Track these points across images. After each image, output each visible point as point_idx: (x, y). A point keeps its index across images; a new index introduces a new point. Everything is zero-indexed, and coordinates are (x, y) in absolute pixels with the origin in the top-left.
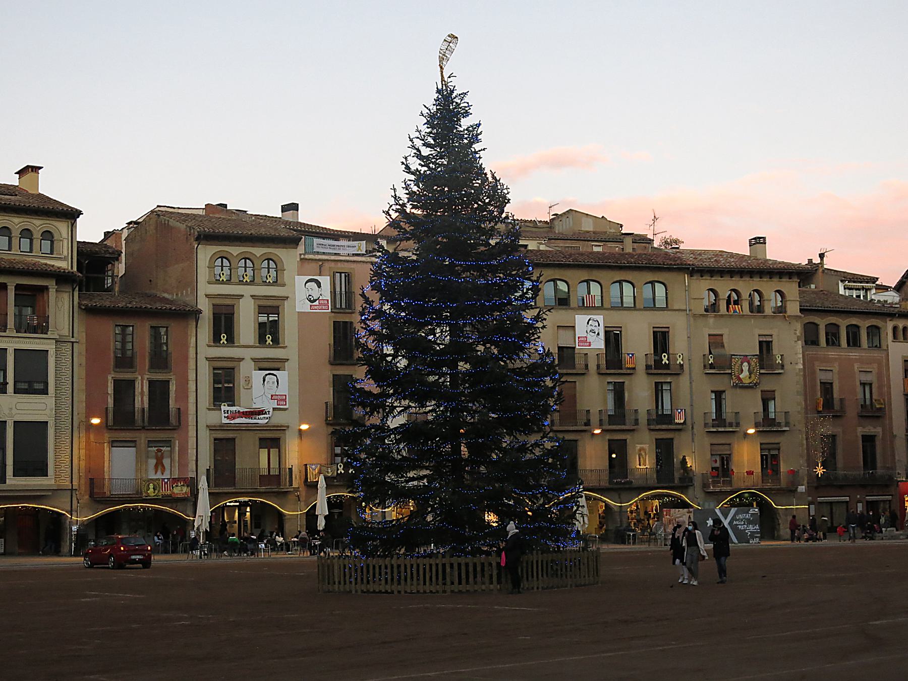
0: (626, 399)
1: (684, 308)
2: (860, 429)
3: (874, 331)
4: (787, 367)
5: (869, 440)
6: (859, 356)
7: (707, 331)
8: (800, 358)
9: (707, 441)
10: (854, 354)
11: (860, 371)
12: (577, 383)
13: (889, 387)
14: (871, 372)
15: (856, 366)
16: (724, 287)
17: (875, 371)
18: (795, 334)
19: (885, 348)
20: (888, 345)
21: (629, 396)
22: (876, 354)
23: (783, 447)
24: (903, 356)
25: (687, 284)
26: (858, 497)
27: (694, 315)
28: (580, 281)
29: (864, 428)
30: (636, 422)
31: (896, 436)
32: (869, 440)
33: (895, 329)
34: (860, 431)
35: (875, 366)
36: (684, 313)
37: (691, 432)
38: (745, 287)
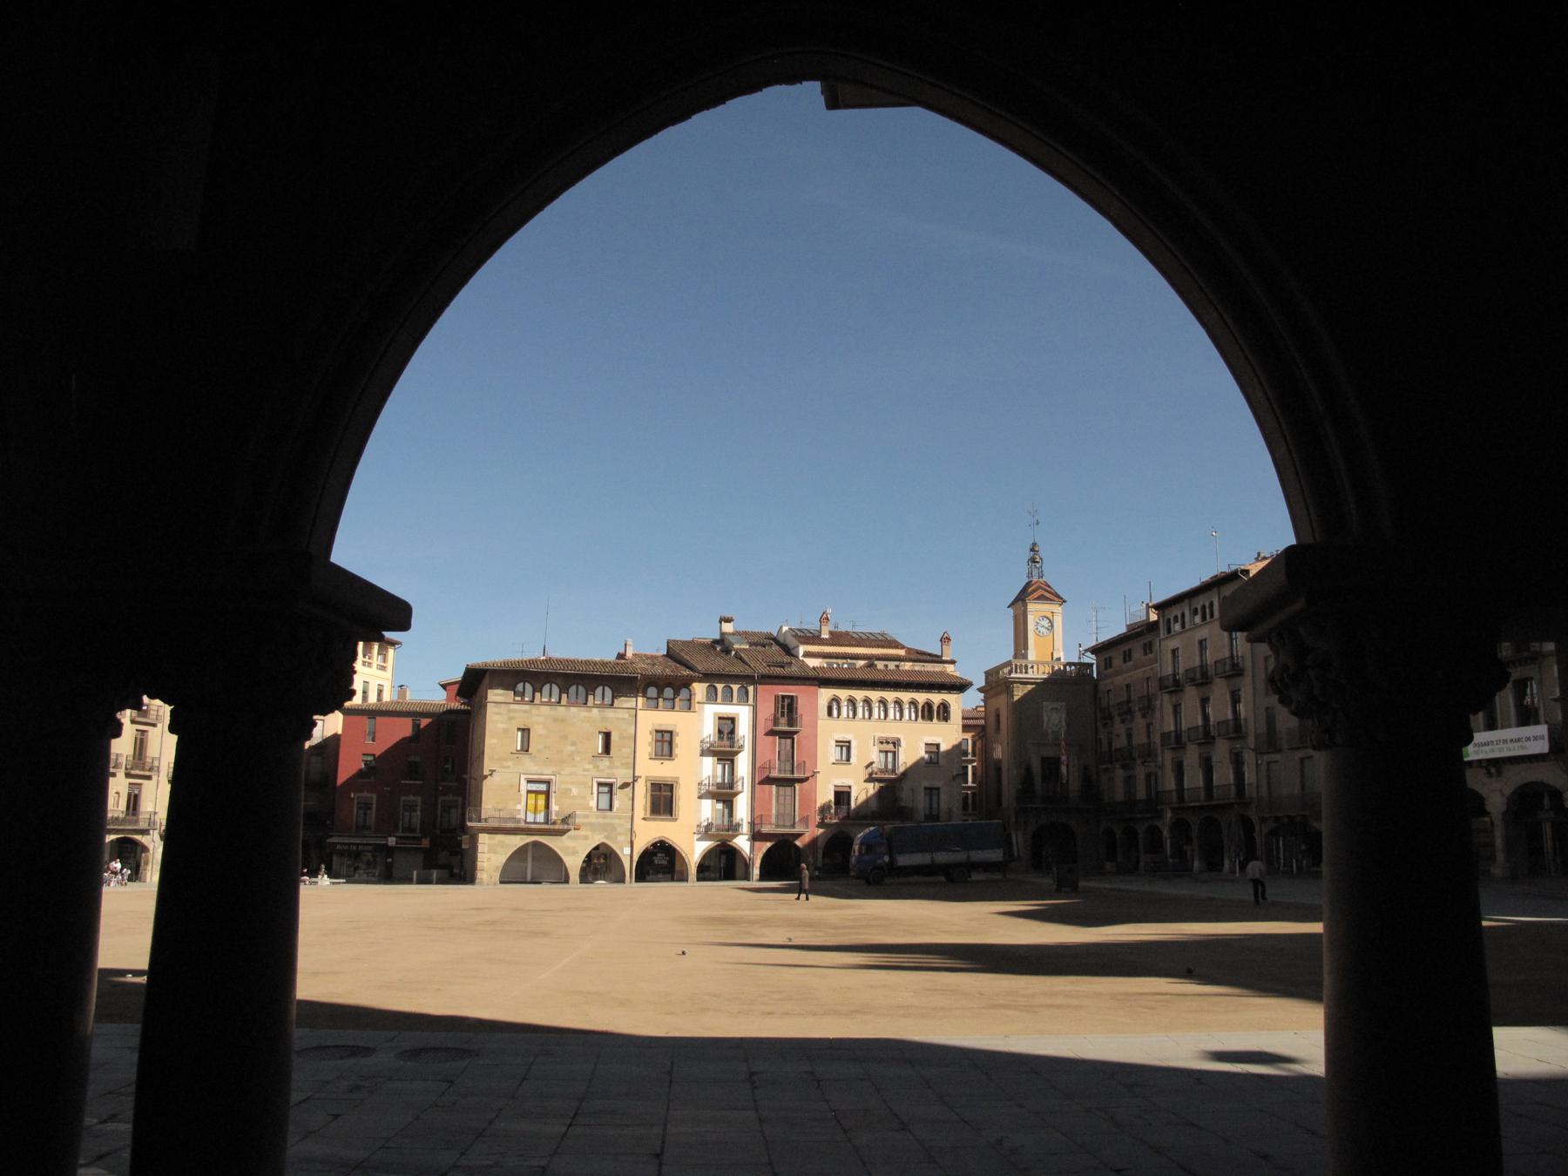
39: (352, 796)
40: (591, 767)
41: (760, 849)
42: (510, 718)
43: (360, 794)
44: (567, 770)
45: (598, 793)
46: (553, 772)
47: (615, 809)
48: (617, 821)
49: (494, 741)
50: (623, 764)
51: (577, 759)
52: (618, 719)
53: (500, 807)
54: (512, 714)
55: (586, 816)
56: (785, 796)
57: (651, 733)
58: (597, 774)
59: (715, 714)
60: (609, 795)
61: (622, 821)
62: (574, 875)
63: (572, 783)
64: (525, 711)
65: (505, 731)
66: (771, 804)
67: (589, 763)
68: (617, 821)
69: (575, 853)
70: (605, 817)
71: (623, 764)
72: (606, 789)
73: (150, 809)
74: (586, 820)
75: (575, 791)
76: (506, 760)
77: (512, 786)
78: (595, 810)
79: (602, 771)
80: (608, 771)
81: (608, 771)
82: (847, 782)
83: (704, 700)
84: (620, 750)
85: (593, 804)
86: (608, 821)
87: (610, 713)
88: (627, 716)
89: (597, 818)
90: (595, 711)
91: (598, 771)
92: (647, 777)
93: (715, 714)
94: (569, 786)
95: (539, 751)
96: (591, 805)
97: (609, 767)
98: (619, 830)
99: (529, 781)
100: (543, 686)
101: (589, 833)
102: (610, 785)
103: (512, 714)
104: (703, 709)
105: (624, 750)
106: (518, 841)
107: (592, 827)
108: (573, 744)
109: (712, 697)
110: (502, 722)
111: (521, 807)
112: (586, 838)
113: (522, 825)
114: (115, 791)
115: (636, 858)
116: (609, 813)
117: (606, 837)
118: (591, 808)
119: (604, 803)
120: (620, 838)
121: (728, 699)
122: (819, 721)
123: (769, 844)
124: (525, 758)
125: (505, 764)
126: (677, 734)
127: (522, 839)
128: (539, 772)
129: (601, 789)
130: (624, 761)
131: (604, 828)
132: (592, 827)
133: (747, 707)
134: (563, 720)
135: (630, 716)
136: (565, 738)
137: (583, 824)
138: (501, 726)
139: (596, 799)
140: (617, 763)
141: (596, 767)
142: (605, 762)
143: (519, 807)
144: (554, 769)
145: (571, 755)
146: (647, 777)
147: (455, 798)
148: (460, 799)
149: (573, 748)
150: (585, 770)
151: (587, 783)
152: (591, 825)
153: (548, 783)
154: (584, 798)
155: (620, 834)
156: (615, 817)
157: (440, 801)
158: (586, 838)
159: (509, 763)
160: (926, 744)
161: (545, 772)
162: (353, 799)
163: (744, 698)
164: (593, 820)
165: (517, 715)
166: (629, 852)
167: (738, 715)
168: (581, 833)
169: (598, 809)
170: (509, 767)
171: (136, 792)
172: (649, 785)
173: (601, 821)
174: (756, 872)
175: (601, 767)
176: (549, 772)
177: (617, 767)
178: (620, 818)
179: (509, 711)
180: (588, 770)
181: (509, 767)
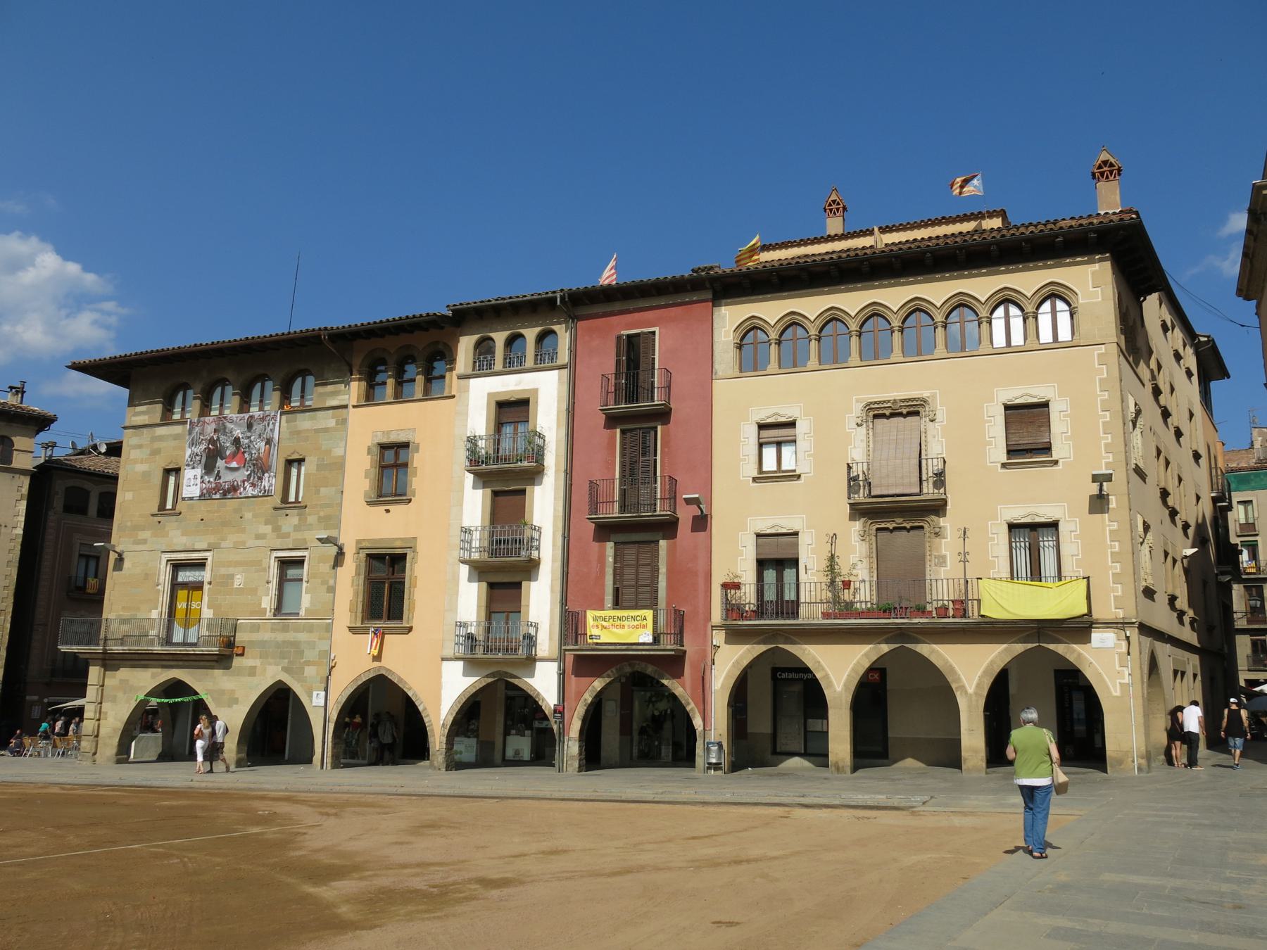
40: (267, 529)
41: (580, 695)
42: (155, 452)
46: (209, 544)
48: (302, 637)
52: (317, 431)
54: (157, 445)
56: (638, 565)
57: (369, 451)
58: (278, 545)
59: (489, 394)
61: (312, 637)
65: (146, 475)
66: (603, 585)
68: (302, 637)
70: (285, 629)
74: (255, 637)
75: (238, 581)
77: (147, 576)
78: (269, 615)
79: (287, 536)
81: (294, 536)
82: (786, 523)
83: (470, 371)
84: (318, 492)
85: (268, 602)
86: (290, 636)
88: (331, 423)
89: (273, 630)
91: (278, 537)
92: (358, 542)
93: (489, 394)
94: (231, 570)
97: (297, 528)
98: (310, 655)
101: (257, 662)
102: (299, 562)
103: (157, 445)
104: (467, 390)
105: (323, 490)
106: (146, 680)
107: (265, 650)
109: (483, 363)
111: (157, 613)
112: (252, 671)
113: (157, 649)
115: (333, 715)
117: (285, 670)
120: (310, 671)
121: (513, 365)
122: (717, 385)
123: (598, 684)
124: (169, 523)
125: (143, 535)
126: (417, 449)
127: (153, 676)
130: (322, 514)
132: (265, 650)
133: (554, 375)
137: (251, 642)
138: (141, 468)
140: (311, 519)
141: (277, 529)
142: (290, 521)
143: (154, 614)
144: (212, 539)
146: (358, 542)
150: (258, 537)
151: (259, 563)
152: (262, 644)
153: (201, 565)
154: (254, 591)
155: (308, 663)
158: (252, 671)
160: (1007, 408)
163: (545, 359)
164: (266, 636)
166: (322, 703)
167: (536, 391)
170: (145, 542)
172: (363, 555)
173: (281, 637)
174: (571, 747)
176: (205, 546)
178: (310, 629)
181: (145, 542)
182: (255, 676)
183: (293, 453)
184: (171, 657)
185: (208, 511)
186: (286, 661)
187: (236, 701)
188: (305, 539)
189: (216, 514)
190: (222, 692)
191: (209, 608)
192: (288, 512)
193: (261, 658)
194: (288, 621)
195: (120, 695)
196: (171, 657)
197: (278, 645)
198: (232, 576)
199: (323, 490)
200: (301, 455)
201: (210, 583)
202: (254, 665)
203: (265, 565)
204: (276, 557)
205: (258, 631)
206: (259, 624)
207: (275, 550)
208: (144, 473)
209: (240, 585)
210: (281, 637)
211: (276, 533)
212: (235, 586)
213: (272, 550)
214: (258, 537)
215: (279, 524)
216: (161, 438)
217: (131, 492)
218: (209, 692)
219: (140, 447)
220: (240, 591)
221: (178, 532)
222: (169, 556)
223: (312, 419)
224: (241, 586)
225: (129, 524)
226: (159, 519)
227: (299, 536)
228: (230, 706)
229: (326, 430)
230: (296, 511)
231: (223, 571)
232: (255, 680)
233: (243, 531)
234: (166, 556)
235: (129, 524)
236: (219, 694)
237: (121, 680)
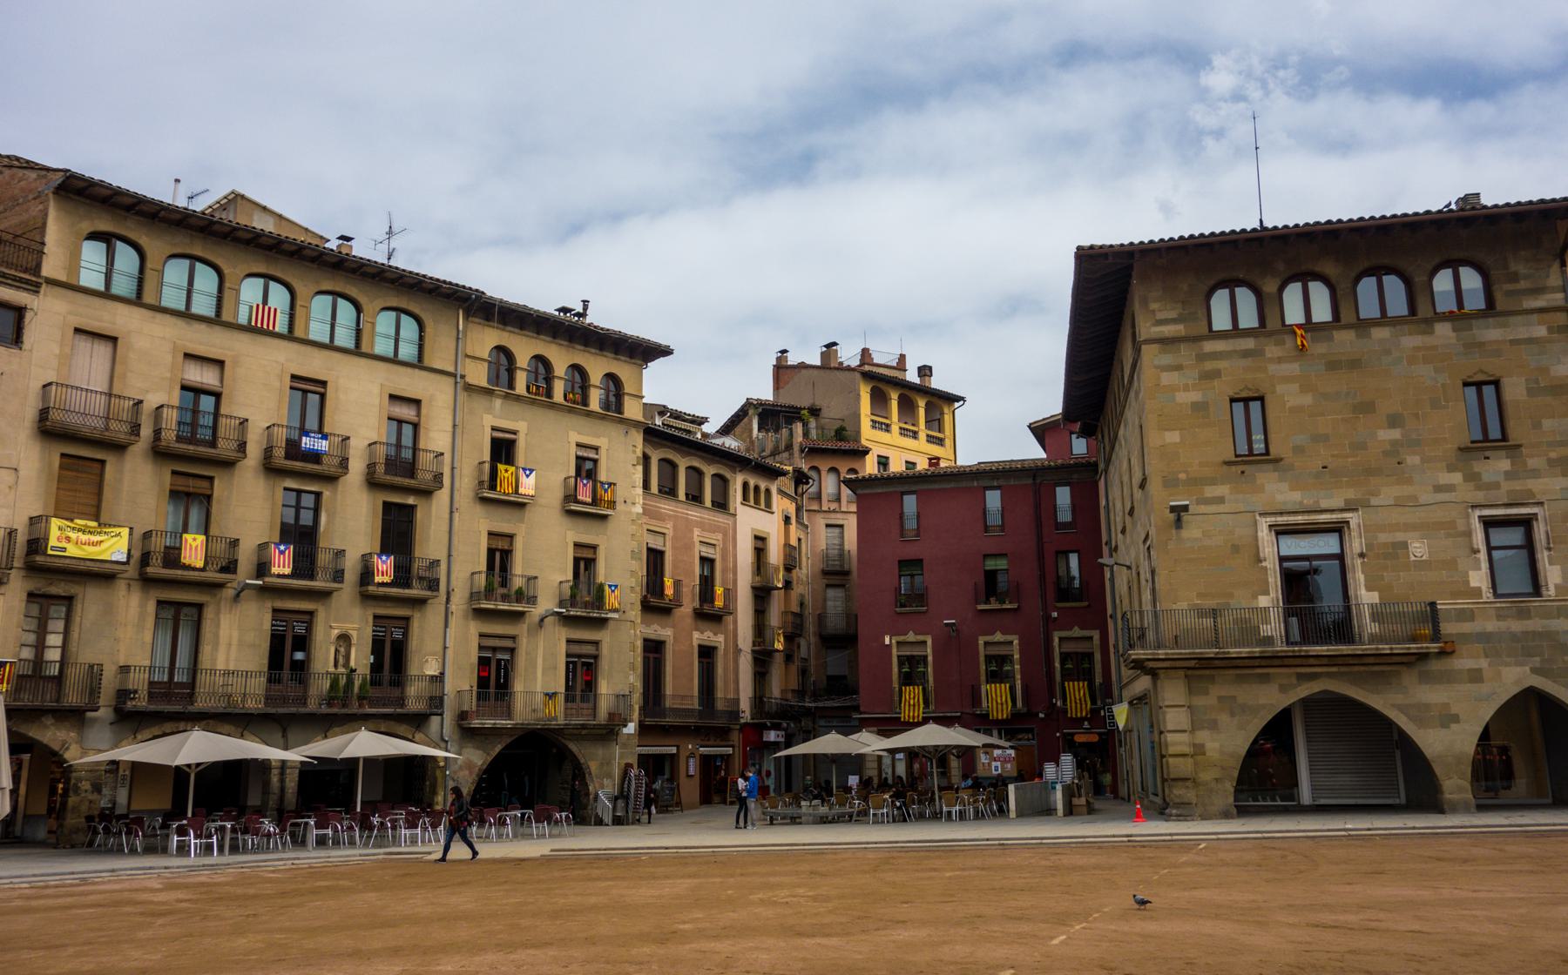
0: (322, 529)
1: (451, 369)
2: (696, 635)
3: (722, 483)
4: (620, 507)
5: (707, 653)
6: (701, 517)
7: (489, 421)
8: (639, 495)
9: (475, 628)
10: (694, 513)
11: (700, 542)
12: (216, 482)
13: (735, 573)
14: (714, 545)
15: (697, 532)
16: (524, 349)
17: (720, 544)
18: (634, 452)
19: (732, 511)
20: (736, 508)
21: (328, 522)
22: (720, 518)
23: (605, 650)
24: (753, 529)
25: (461, 327)
26: (690, 747)
27: (470, 388)
28: (247, 272)
29: (702, 633)
30: (338, 576)
31: (741, 650)
32: (707, 653)
33: (745, 485)
34: (698, 637)
35: (720, 536)
36: (451, 380)
37: (443, 608)
38: (561, 359)
39: (887, 641)
40: (1456, 478)
42: (1216, 374)
43: (901, 638)
44: (1388, 494)
45: (1490, 549)
47: (1551, 592)
49: (1173, 437)
50: (1551, 462)
51: (1413, 460)
53: (1211, 603)
54: (1209, 365)
55: (1465, 615)
58: (1480, 497)
60: (1524, 553)
62: (1455, 785)
63: (1407, 527)
64: (1246, 354)
65: (1199, 408)
67: (1451, 469)
69: (1448, 719)
70: (1524, 614)
71: (1551, 462)
72: (1515, 536)
73: (432, 669)
74: (1466, 627)
75: (1418, 549)
76: (1213, 482)
77: (1236, 549)
78: (1487, 595)
79: (1497, 486)
80: (1506, 486)
81: (1506, 486)
84: (1537, 425)
85: (1479, 578)
87: (1491, 333)
88: (1541, 331)
90: (1443, 330)
91: (1478, 488)
94: (1400, 536)
95: (1299, 450)
96: (1474, 583)
97: (1509, 475)
99: (1281, 531)
100: (1281, 289)
101: (1483, 663)
102: (1526, 523)
103: (1209, 365)
105: (1547, 424)
108: (1394, 421)
110: (1186, 388)
112: (1476, 676)
114: (336, 632)
116: (1535, 603)
117: (1534, 671)
118: (1477, 592)
119: (1516, 580)
125: (1211, 491)
128: (1308, 502)
129: (1501, 537)
130: (1553, 455)
131: (1523, 647)
134: (1355, 364)
135: (1550, 330)
136: (1366, 408)
137: (1466, 638)
139: (1485, 565)
140: (1532, 463)
141: (1472, 477)
142: (1497, 467)
143: (1263, 601)
144: (1351, 494)
145: (1394, 450)
147: (1086, 633)
148: (1096, 635)
149: (1395, 434)
150: (1439, 489)
152: (1484, 637)
153: (1338, 529)
154: (1451, 564)
156: (1547, 614)
157: (1056, 640)
158: (1476, 676)
159: (1222, 490)
161: (1324, 504)
162: (890, 646)
164: (1491, 626)
165: (1222, 365)
168: (1463, 662)
169: (1496, 595)
170: (1220, 500)
171: (398, 635)
173: (1516, 626)
175: (1487, 477)
176: (1342, 505)
177: (1535, 473)
179: (1202, 357)
180: (1450, 488)
181: (1220, 500)
182: (1483, 682)
183: (1475, 374)
184: (1325, 661)
185: (1333, 456)
186: (1538, 659)
187: (1455, 719)
188: (1530, 490)
189: (1350, 460)
190: (1427, 706)
191: (1369, 589)
192: (1487, 453)
193: (1487, 656)
194: (1529, 604)
195: (1224, 718)
196: (1325, 661)
197: (1514, 637)
198: (1404, 545)
199: (1547, 424)
200: (1492, 376)
201: (1362, 555)
202: (1477, 667)
203: (1461, 527)
204: (1479, 517)
205: (1473, 620)
206: (1472, 610)
207: (1476, 506)
208: (1196, 407)
209: (1422, 557)
210: (1516, 626)
211: (1472, 484)
212: (1413, 558)
213: (1472, 506)
214: (1439, 489)
215: (1476, 470)
216: (1215, 356)
217: (1177, 433)
218: (1402, 709)
219: (1179, 368)
220: (1421, 565)
221: (1284, 486)
222: (1273, 519)
223: (1505, 326)
224: (1424, 558)
225: (1182, 476)
226: (1240, 468)
227: (1517, 485)
228: (1444, 725)
229: (1531, 341)
230: (1503, 453)
231: (1383, 538)
232: (1485, 688)
233: (1409, 481)
234: (1268, 519)
235: (1182, 476)
236: (1422, 714)
237: (1220, 699)
